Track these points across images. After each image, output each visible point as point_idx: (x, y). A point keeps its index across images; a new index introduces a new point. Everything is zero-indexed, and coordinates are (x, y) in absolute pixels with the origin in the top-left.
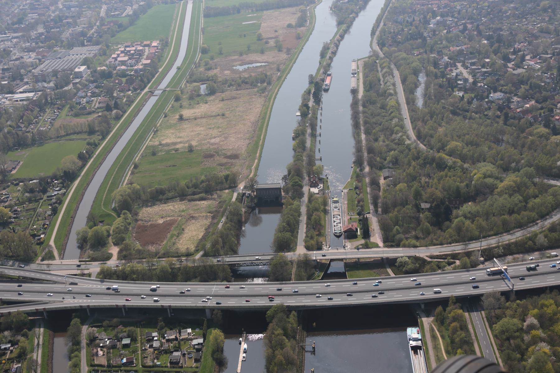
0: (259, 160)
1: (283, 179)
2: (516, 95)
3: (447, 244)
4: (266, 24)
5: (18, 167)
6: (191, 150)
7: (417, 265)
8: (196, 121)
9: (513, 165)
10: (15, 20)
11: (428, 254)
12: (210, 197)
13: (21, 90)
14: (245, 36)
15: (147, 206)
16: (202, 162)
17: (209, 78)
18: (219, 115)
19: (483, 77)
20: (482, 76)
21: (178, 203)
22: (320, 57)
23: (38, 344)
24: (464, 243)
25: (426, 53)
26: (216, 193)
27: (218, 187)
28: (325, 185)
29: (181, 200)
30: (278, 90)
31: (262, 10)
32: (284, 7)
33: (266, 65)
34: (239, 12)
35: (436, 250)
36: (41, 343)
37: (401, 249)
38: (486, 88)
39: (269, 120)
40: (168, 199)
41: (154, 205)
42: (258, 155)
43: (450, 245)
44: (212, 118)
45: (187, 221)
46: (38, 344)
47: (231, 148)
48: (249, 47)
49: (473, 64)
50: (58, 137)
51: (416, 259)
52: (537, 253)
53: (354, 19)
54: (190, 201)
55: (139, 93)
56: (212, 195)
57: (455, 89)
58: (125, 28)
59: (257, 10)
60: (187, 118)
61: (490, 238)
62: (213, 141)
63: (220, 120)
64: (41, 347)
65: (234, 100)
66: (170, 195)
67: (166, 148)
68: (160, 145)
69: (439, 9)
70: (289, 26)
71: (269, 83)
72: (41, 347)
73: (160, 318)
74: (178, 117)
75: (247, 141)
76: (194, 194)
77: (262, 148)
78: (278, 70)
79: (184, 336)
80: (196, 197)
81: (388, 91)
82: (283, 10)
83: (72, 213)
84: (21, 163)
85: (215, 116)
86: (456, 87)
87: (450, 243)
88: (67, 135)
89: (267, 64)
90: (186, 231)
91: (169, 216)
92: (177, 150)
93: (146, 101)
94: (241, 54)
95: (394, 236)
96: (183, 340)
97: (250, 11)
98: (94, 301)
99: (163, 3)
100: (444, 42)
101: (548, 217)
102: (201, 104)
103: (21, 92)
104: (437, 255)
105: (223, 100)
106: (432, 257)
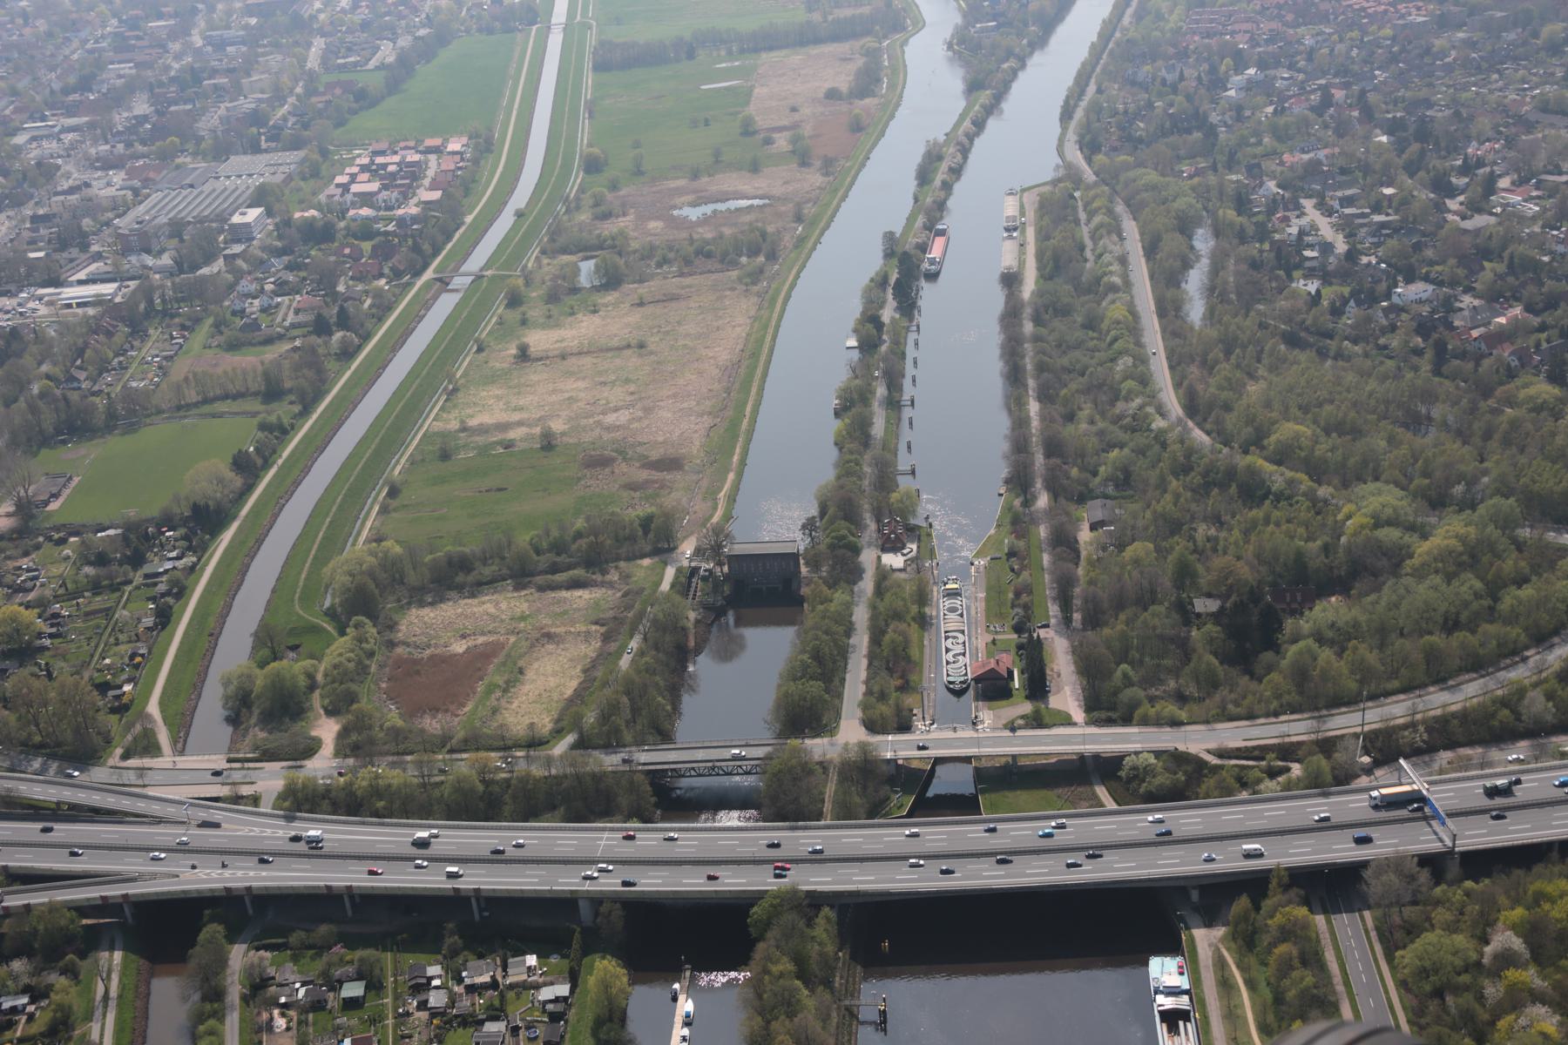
0: (740, 475)
1: (804, 527)
2: (1469, 290)
3: (1267, 715)
4: (765, 90)
5: (66, 492)
6: (548, 443)
7: (1181, 777)
8: (565, 362)
9: (1459, 489)
10: (72, 80)
11: (1213, 745)
12: (598, 577)
13: (82, 275)
14: (707, 122)
16: (579, 479)
17: (605, 241)
18: (629, 346)
19: (1376, 240)
20: (1374, 236)
21: (510, 595)
22: (916, 183)
23: (106, 997)
24: (1317, 714)
25: (1215, 169)
26: (617, 567)
27: (623, 551)
28: (923, 544)
29: (518, 587)
30: (797, 276)
32: (818, 41)
33: (764, 205)
34: (691, 55)
35: (1234, 735)
36: (114, 992)
37: (1134, 730)
38: (1383, 271)
39: (768, 361)
40: (480, 584)
41: (441, 601)
42: (736, 458)
43: (1274, 720)
44: (609, 355)
45: (532, 646)
46: (106, 997)
47: (661, 439)
48: (717, 154)
49: (1348, 201)
50: (179, 408)
51: (1178, 759)
52: (1523, 744)
53: (1014, 74)
54: (541, 589)
55: (409, 285)
56: (604, 572)
57: (1296, 274)
58: (374, 103)
59: (742, 51)
60: (540, 354)
61: (1394, 698)
62: (610, 419)
63: (632, 360)
64: (112, 1004)
65: (674, 305)
66: (487, 571)
67: (480, 440)
68: (464, 429)
69: (1253, 47)
70: (832, 95)
71: (772, 256)
72: (112, 1004)
73: (451, 926)
74: (514, 351)
75: (707, 421)
76: (554, 569)
77: (749, 440)
78: (799, 218)
79: (516, 976)
81: (1106, 279)
82: (815, 50)
83: (211, 622)
84: (76, 480)
85: (619, 349)
86: (1298, 266)
87: (1276, 715)
88: (206, 401)
89: (767, 201)
90: (530, 675)
91: (483, 634)
92: (508, 445)
93: (427, 306)
94: (695, 176)
95: (1115, 694)
96: (512, 986)
97: (723, 53)
98: (264, 874)
99: (480, 30)
100: (1266, 140)
101: (1556, 640)
102: (580, 316)
103: (81, 282)
104: (1238, 749)
105: (641, 304)
106: (1222, 753)
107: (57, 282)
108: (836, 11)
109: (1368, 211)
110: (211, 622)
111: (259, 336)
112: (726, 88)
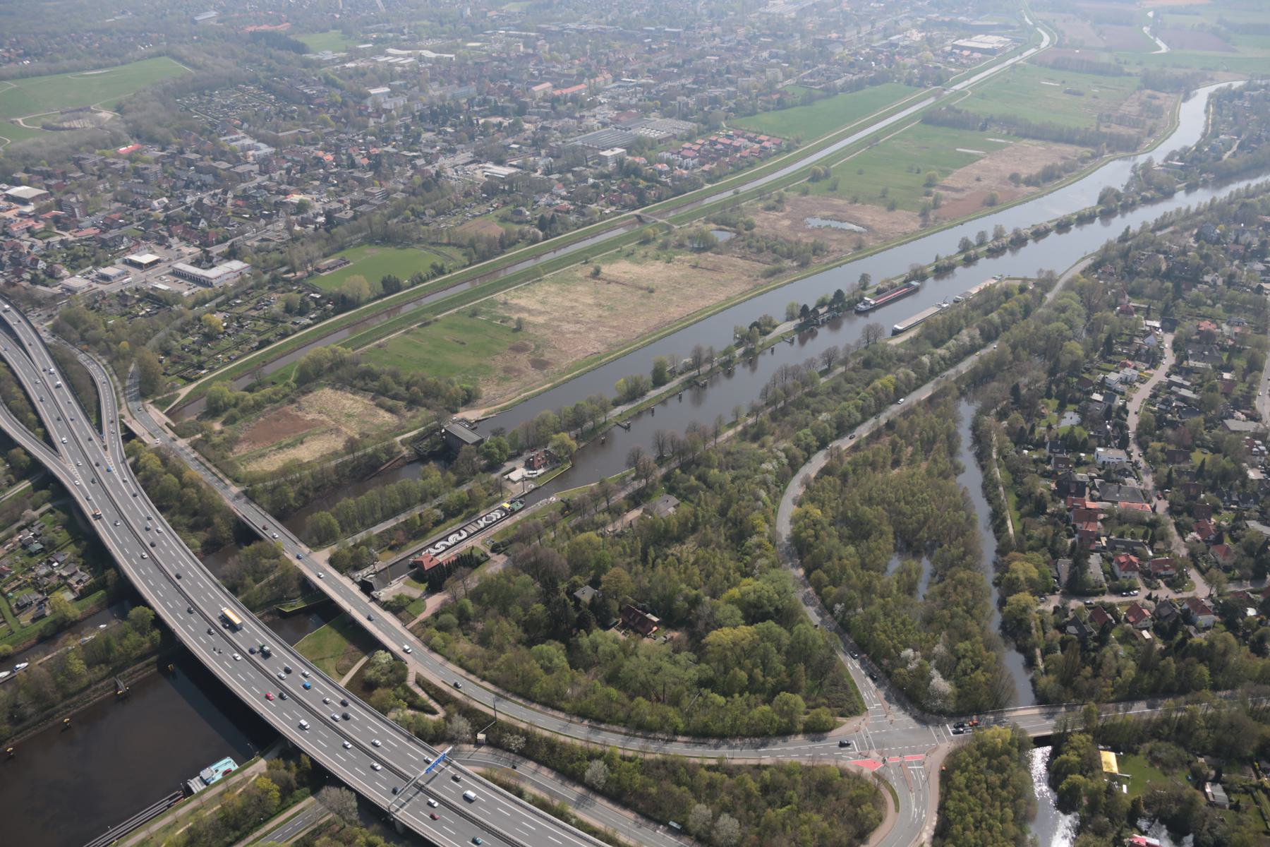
3: (479, 677)
7: (383, 679)
9: (838, 607)
12: (404, 411)
13: (515, 163)
14: (918, 172)
15: (333, 387)
24: (501, 693)
27: (429, 401)
29: (373, 399)
31: (1025, 136)
32: (1069, 141)
34: (983, 129)
43: (478, 681)
48: (884, 194)
50: (433, 244)
51: (398, 666)
52: (579, 790)
57: (1070, 407)
59: (1017, 135)
61: (556, 713)
62: (566, 327)
65: (708, 274)
68: (505, 303)
70: (1015, 178)
71: (804, 265)
75: (602, 348)
76: (394, 397)
79: (72, 581)
80: (390, 402)
85: (641, 288)
86: (1077, 402)
87: (484, 679)
88: (448, 244)
92: (504, 320)
97: (1005, 132)
101: (713, 742)
102: (658, 263)
105: (694, 267)
106: (420, 682)
107: (500, 163)
108: (1113, 125)
109: (1188, 384)
110: (272, 357)
111: (517, 218)
112: (968, 155)
